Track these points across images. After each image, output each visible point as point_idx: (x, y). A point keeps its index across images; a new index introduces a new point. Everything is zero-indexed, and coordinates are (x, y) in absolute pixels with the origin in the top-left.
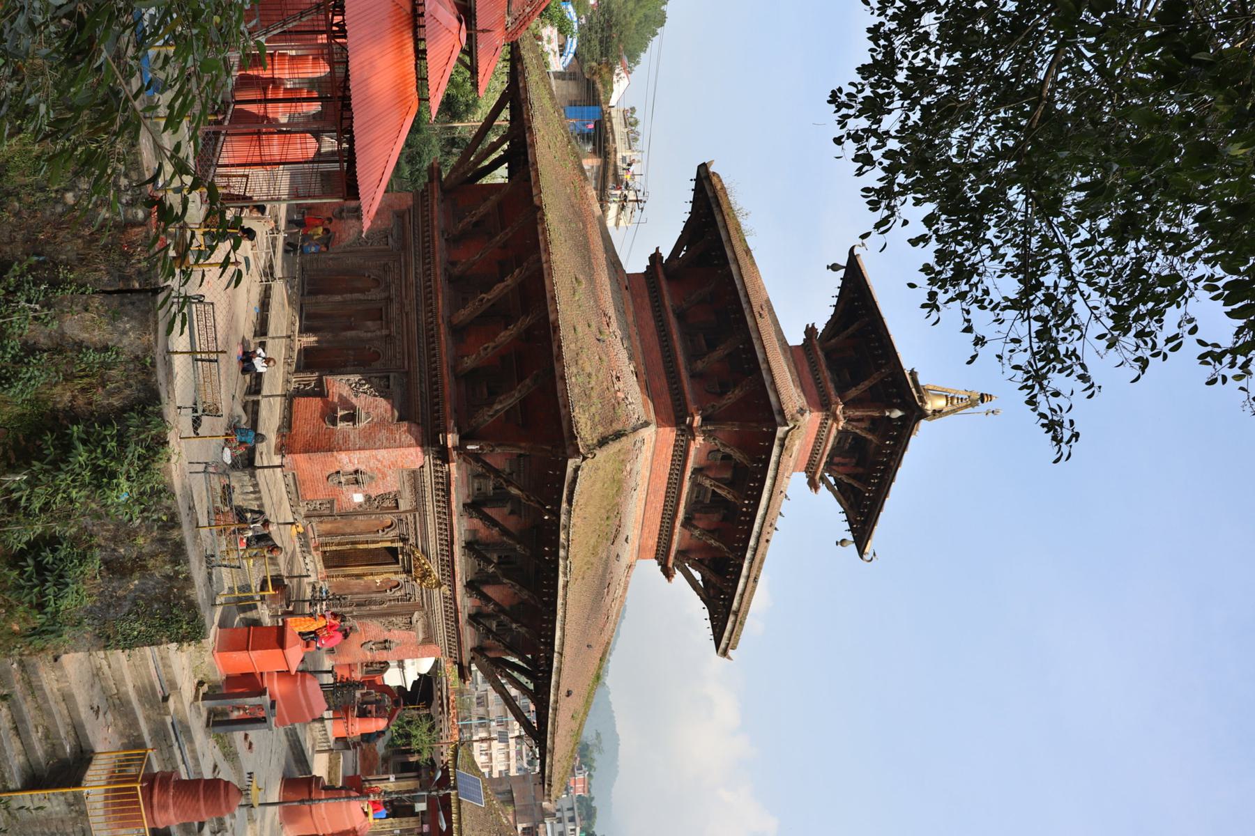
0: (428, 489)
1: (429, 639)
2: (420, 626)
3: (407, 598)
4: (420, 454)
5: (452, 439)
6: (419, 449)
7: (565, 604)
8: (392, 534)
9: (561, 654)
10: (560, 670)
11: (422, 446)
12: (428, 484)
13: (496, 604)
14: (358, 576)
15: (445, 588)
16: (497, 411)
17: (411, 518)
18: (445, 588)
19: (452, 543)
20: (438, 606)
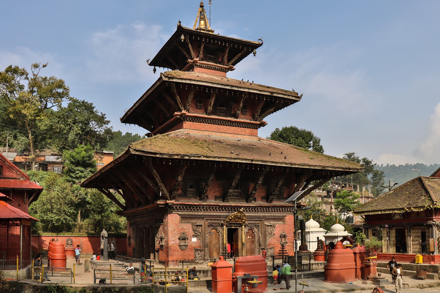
0: (191, 213)
1: (281, 219)
2: (272, 223)
3: (257, 226)
4: (172, 215)
5: (160, 202)
6: (169, 215)
7: (219, 158)
8: (219, 229)
9: (252, 160)
10: (262, 161)
11: (168, 214)
12: (188, 213)
13: (253, 190)
14: (243, 244)
15: (241, 210)
16: (153, 185)
17: (209, 221)
18: (241, 210)
19: (219, 205)
20: (261, 214)
